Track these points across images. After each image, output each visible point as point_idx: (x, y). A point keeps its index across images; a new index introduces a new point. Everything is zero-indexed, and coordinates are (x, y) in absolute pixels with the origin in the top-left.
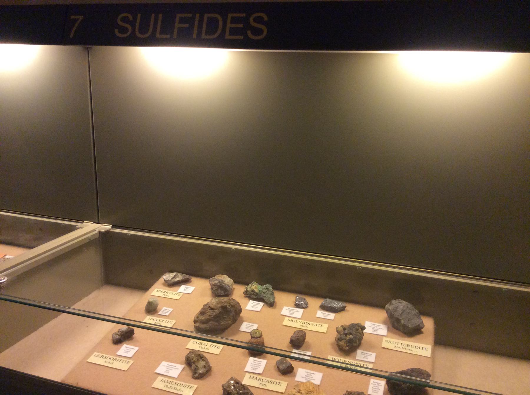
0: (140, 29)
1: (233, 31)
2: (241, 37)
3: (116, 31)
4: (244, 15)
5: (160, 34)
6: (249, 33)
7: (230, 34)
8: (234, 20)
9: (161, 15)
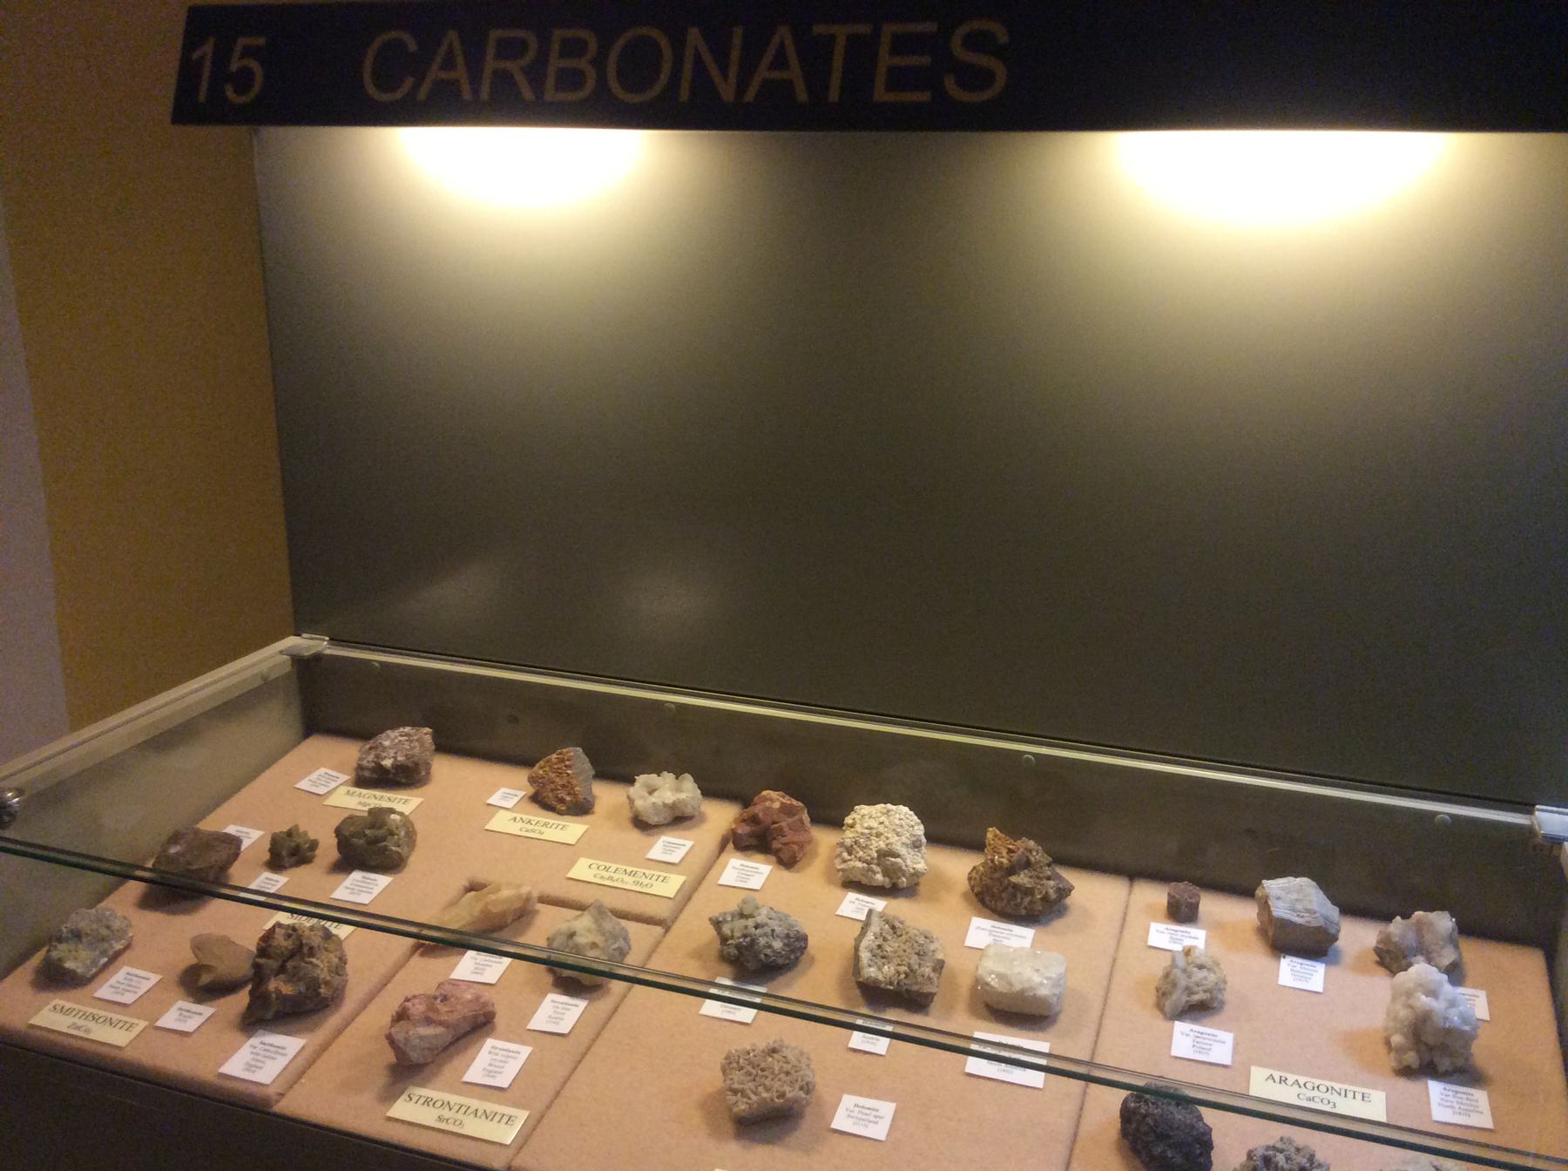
0: (376, 75)
7: (889, 87)
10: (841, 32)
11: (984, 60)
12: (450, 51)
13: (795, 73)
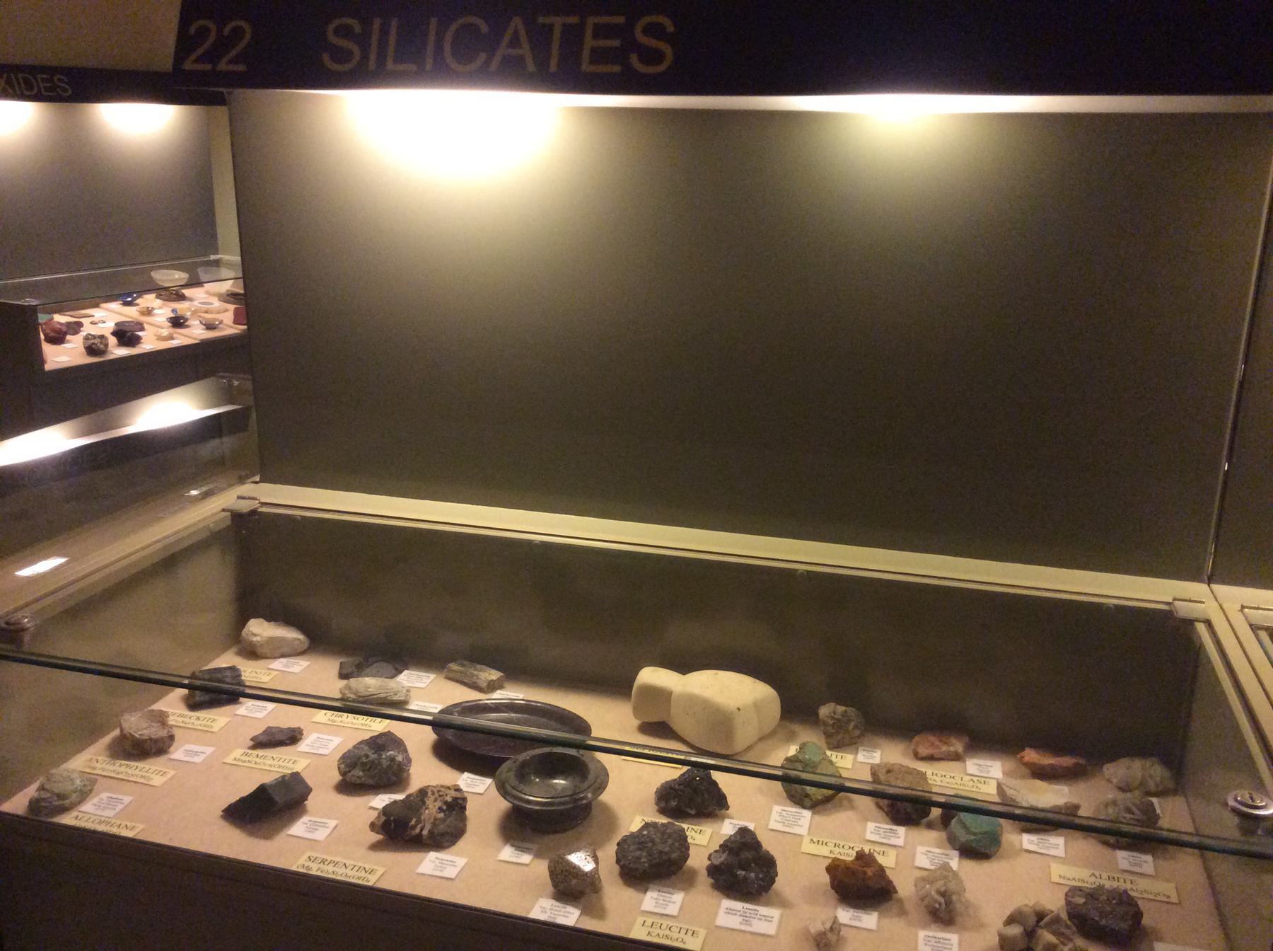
1: (599, 56)
2: (617, 69)
4: (620, 20)
5: (395, 62)
6: (634, 59)
7: (592, 62)
8: (599, 32)
9: (394, 23)
10: (558, 22)
13: (525, 50)
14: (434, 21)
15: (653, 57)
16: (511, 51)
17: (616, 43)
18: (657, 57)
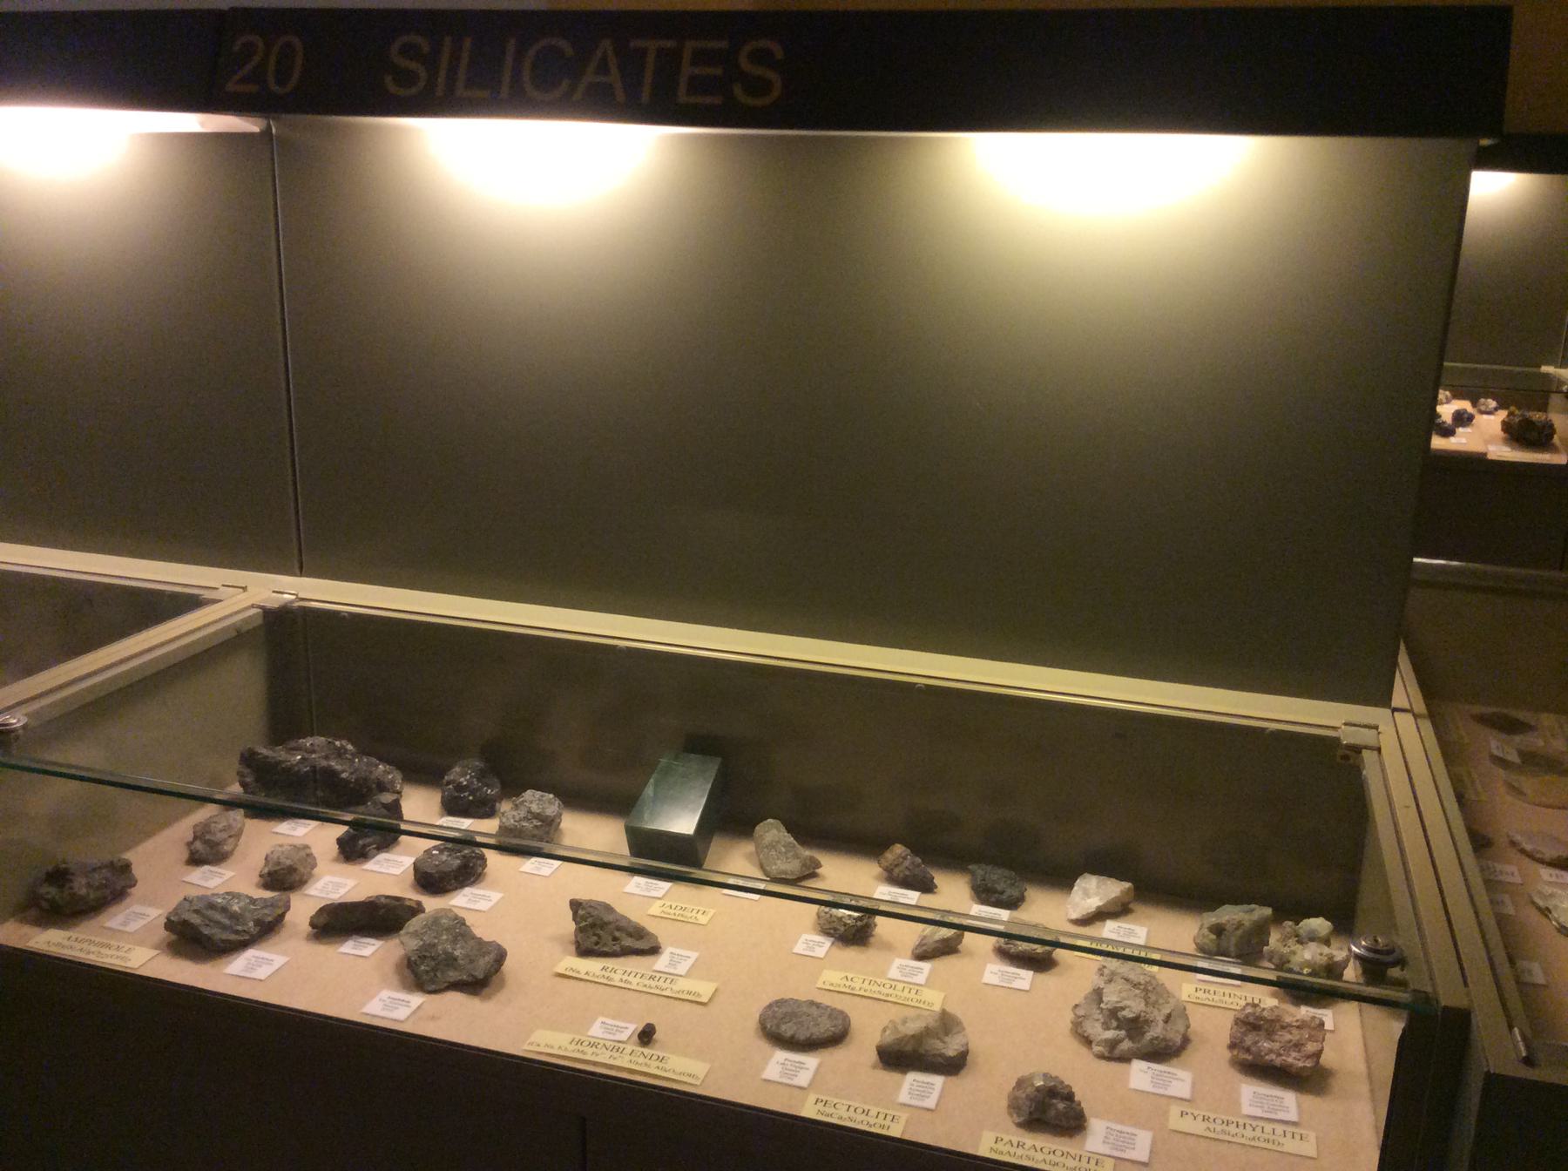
1: (696, 85)
2: (716, 100)
3: (388, 79)
4: (723, 44)
6: (738, 90)
8: (700, 57)
9: (468, 43)
11: (758, 71)
12: (604, 59)
13: (614, 77)
14: (511, 45)
15: (758, 87)
16: (601, 79)
17: (719, 71)
18: (765, 87)
